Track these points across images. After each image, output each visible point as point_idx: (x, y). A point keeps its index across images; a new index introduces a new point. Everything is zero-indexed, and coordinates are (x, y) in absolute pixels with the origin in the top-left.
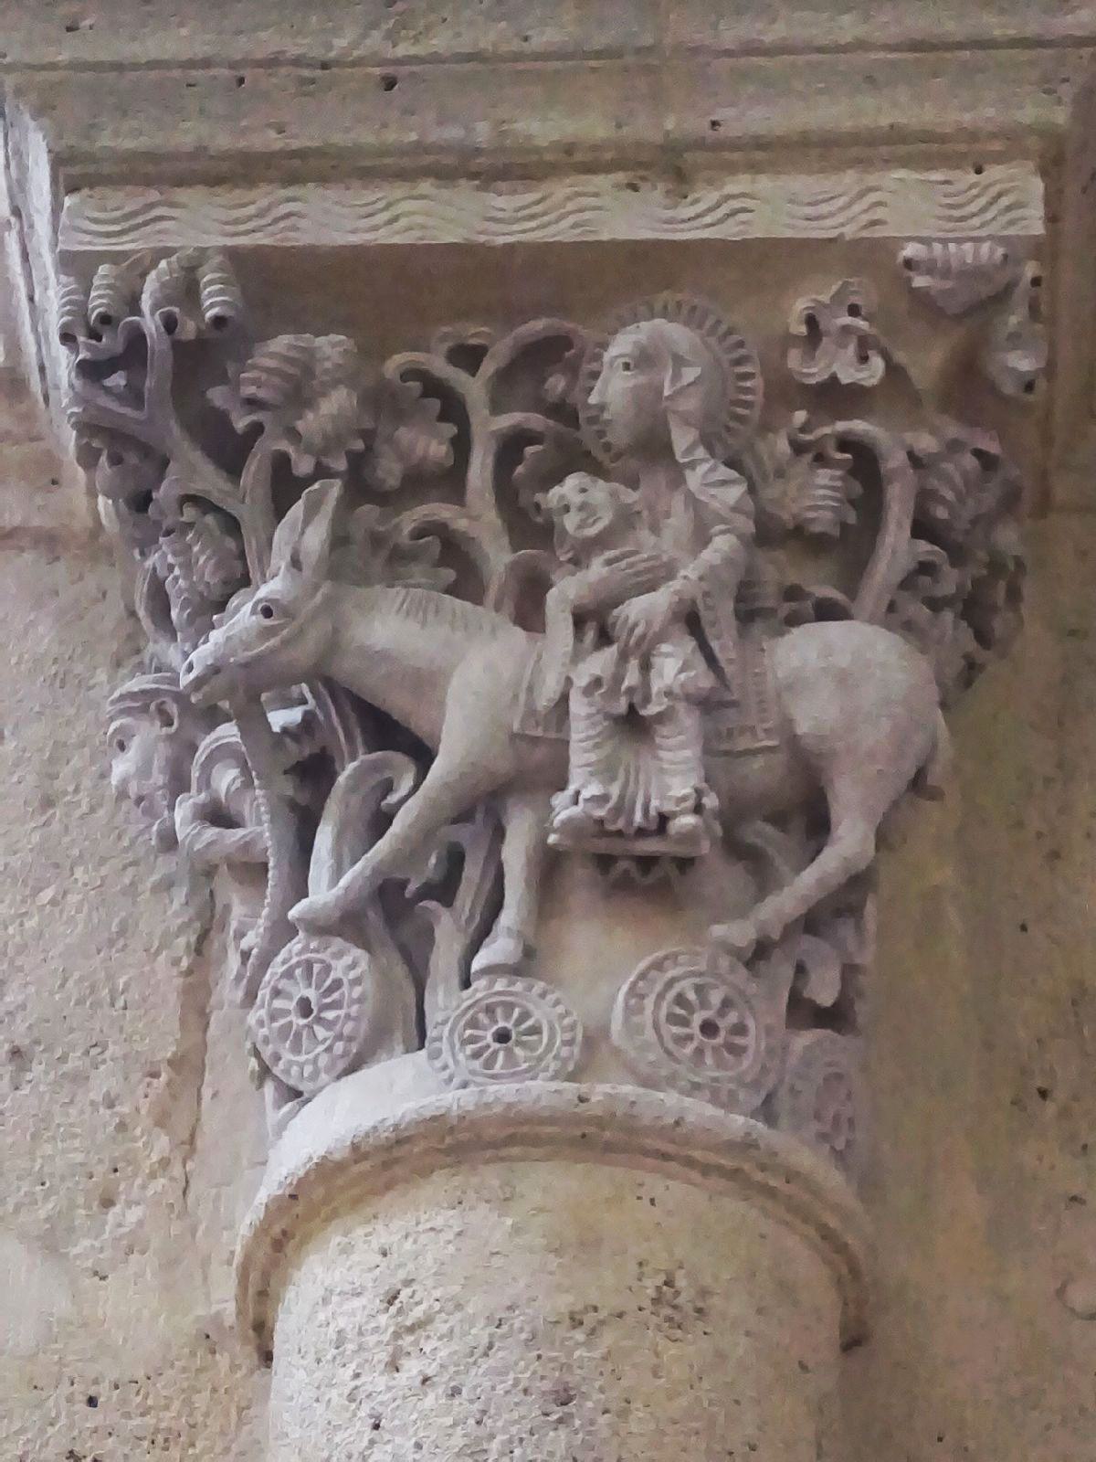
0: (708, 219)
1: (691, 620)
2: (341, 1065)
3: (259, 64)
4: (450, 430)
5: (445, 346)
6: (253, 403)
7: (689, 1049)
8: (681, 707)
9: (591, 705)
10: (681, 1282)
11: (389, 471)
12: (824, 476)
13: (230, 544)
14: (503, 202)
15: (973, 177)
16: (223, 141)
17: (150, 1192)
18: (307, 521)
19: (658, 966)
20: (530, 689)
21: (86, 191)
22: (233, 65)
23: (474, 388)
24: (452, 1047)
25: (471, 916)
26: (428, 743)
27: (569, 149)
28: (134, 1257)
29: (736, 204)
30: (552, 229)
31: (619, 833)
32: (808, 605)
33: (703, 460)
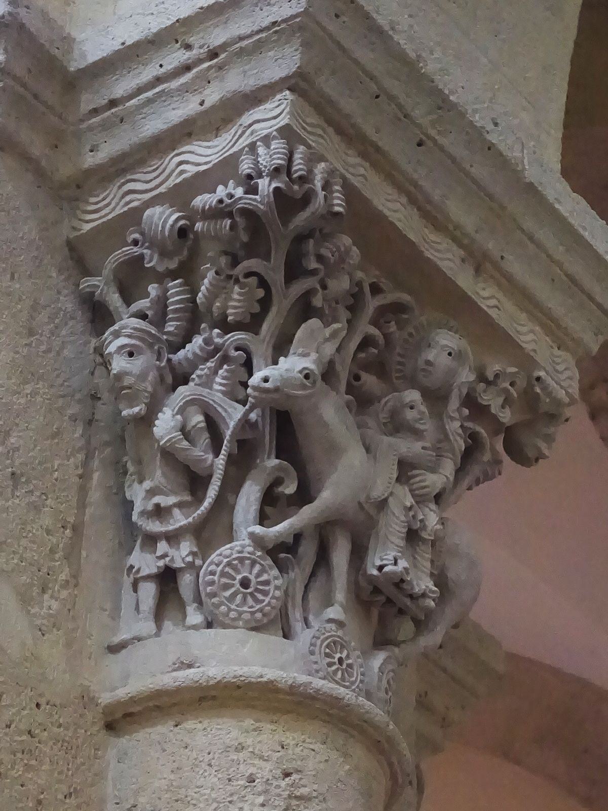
2: (254, 624)
6: (320, 258)
13: (257, 309)
27: (457, 227)
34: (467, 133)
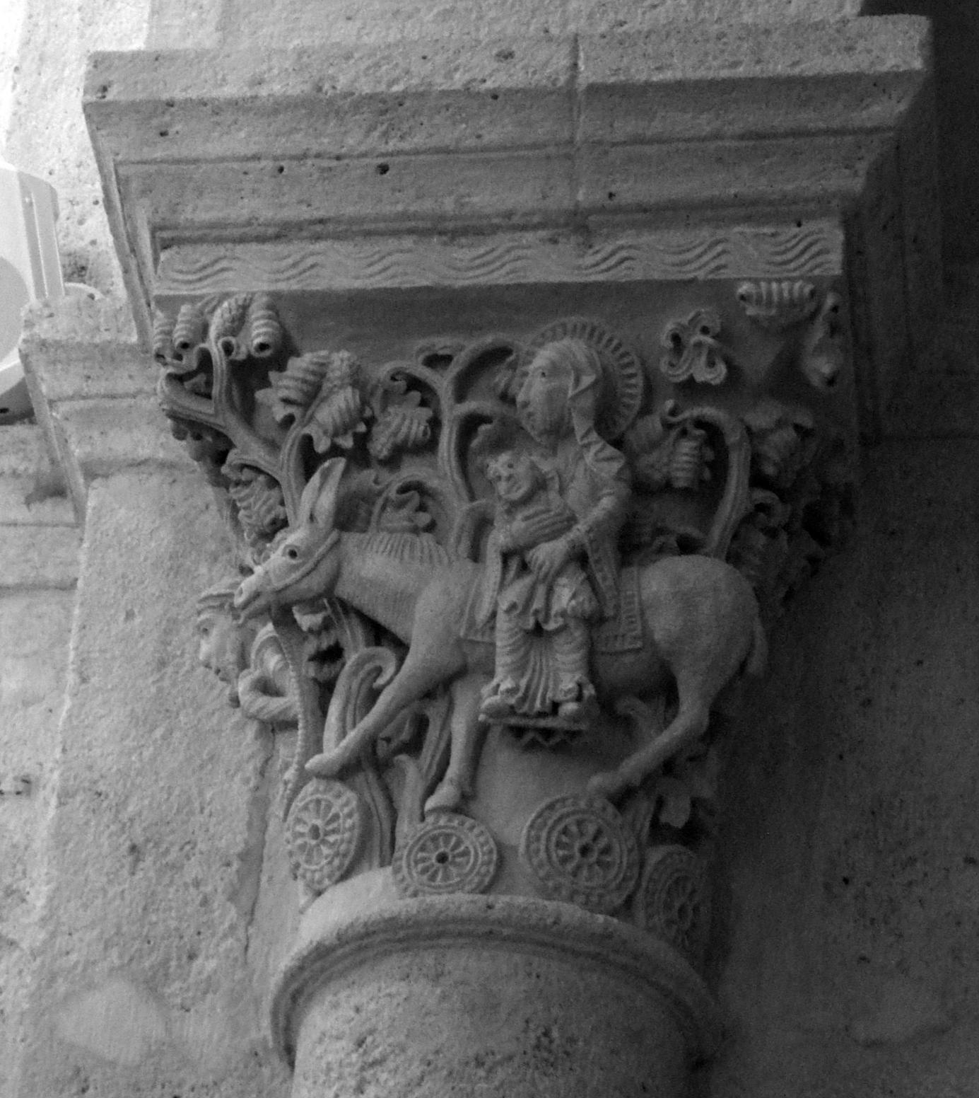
0: (603, 266)
1: (579, 558)
2: (338, 874)
3: (293, 158)
4: (426, 413)
5: (421, 358)
7: (570, 867)
8: (572, 624)
9: (510, 621)
10: (555, 1034)
11: (381, 445)
12: (687, 446)
14: (463, 254)
15: (795, 230)
16: (267, 214)
17: (221, 950)
18: (320, 489)
19: (551, 807)
20: (473, 607)
21: (175, 248)
22: (276, 159)
23: (443, 383)
24: (409, 866)
25: (430, 766)
26: (406, 642)
27: (509, 215)
28: (210, 996)
29: (624, 254)
30: (495, 275)
31: (525, 715)
32: (672, 541)
33: (596, 442)
34: (447, 107)
